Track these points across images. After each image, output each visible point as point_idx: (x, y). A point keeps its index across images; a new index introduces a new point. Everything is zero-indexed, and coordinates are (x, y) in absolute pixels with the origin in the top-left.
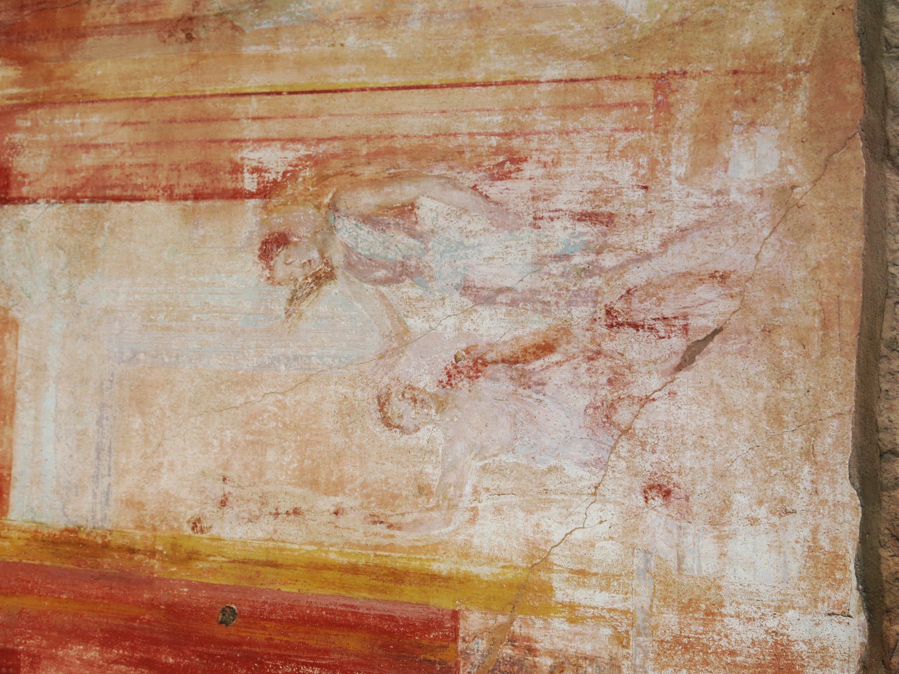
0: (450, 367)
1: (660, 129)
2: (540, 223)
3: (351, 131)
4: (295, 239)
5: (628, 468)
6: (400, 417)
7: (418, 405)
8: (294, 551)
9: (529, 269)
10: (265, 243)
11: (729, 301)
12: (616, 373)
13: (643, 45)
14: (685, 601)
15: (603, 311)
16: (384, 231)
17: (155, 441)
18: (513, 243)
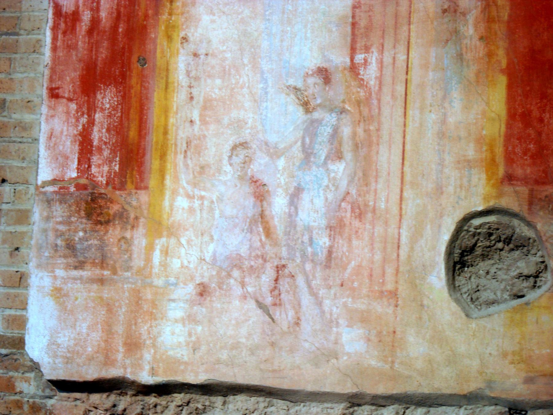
0: (260, 182)
1: (370, 294)
2: (328, 230)
3: (383, 119)
4: (327, 89)
5: (212, 275)
6: (237, 156)
7: (242, 165)
8: (173, 98)
9: (306, 224)
10: (326, 70)
11: (287, 326)
12: (255, 269)
13: (413, 285)
14: (157, 303)
15: (284, 263)
16: (329, 141)
17: (225, 10)
18: (319, 215)
